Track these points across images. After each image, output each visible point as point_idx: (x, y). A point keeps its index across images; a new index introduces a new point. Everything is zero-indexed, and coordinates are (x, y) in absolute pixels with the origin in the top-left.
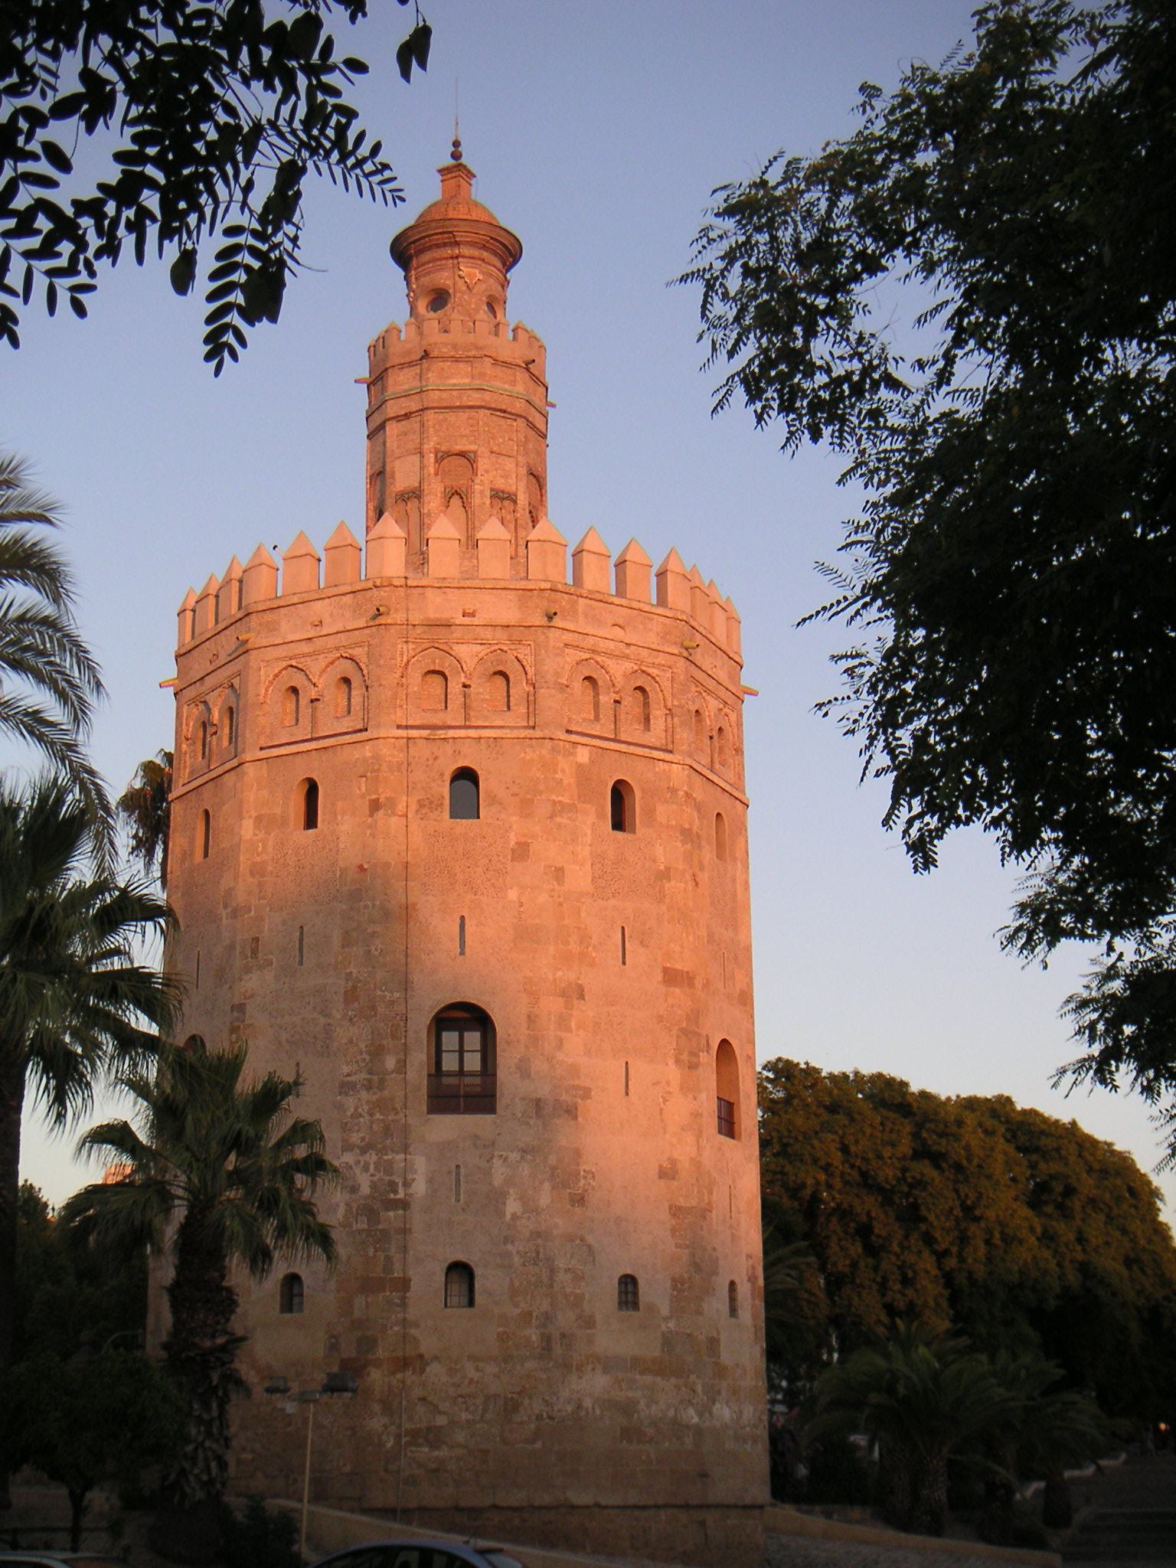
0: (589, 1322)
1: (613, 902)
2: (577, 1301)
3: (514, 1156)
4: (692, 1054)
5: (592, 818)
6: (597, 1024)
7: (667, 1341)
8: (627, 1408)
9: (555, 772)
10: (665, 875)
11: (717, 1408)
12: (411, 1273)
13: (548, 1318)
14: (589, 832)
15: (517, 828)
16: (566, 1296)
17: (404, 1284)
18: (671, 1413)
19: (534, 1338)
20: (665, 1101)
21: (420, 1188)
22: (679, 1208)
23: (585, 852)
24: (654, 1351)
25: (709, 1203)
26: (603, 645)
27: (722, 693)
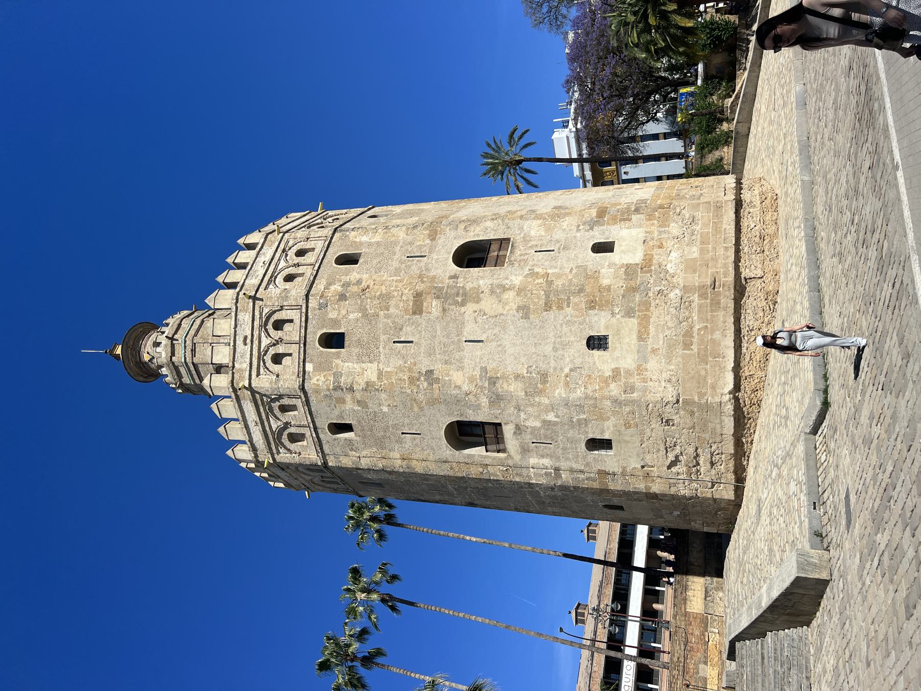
0: (616, 373)
1: (381, 349)
2: (606, 381)
3: (522, 415)
4: (458, 295)
5: (338, 361)
6: (446, 363)
7: (629, 313)
8: (671, 347)
9: (318, 385)
10: (363, 310)
11: (671, 268)
12: (595, 469)
13: (615, 401)
14: (346, 364)
15: (350, 405)
16: (601, 389)
17: (600, 472)
18: (673, 311)
19: (628, 409)
20: (485, 314)
21: (546, 462)
22: (546, 304)
23: (357, 367)
24: (633, 322)
25: (543, 276)
26: (255, 353)
27: (277, 255)
